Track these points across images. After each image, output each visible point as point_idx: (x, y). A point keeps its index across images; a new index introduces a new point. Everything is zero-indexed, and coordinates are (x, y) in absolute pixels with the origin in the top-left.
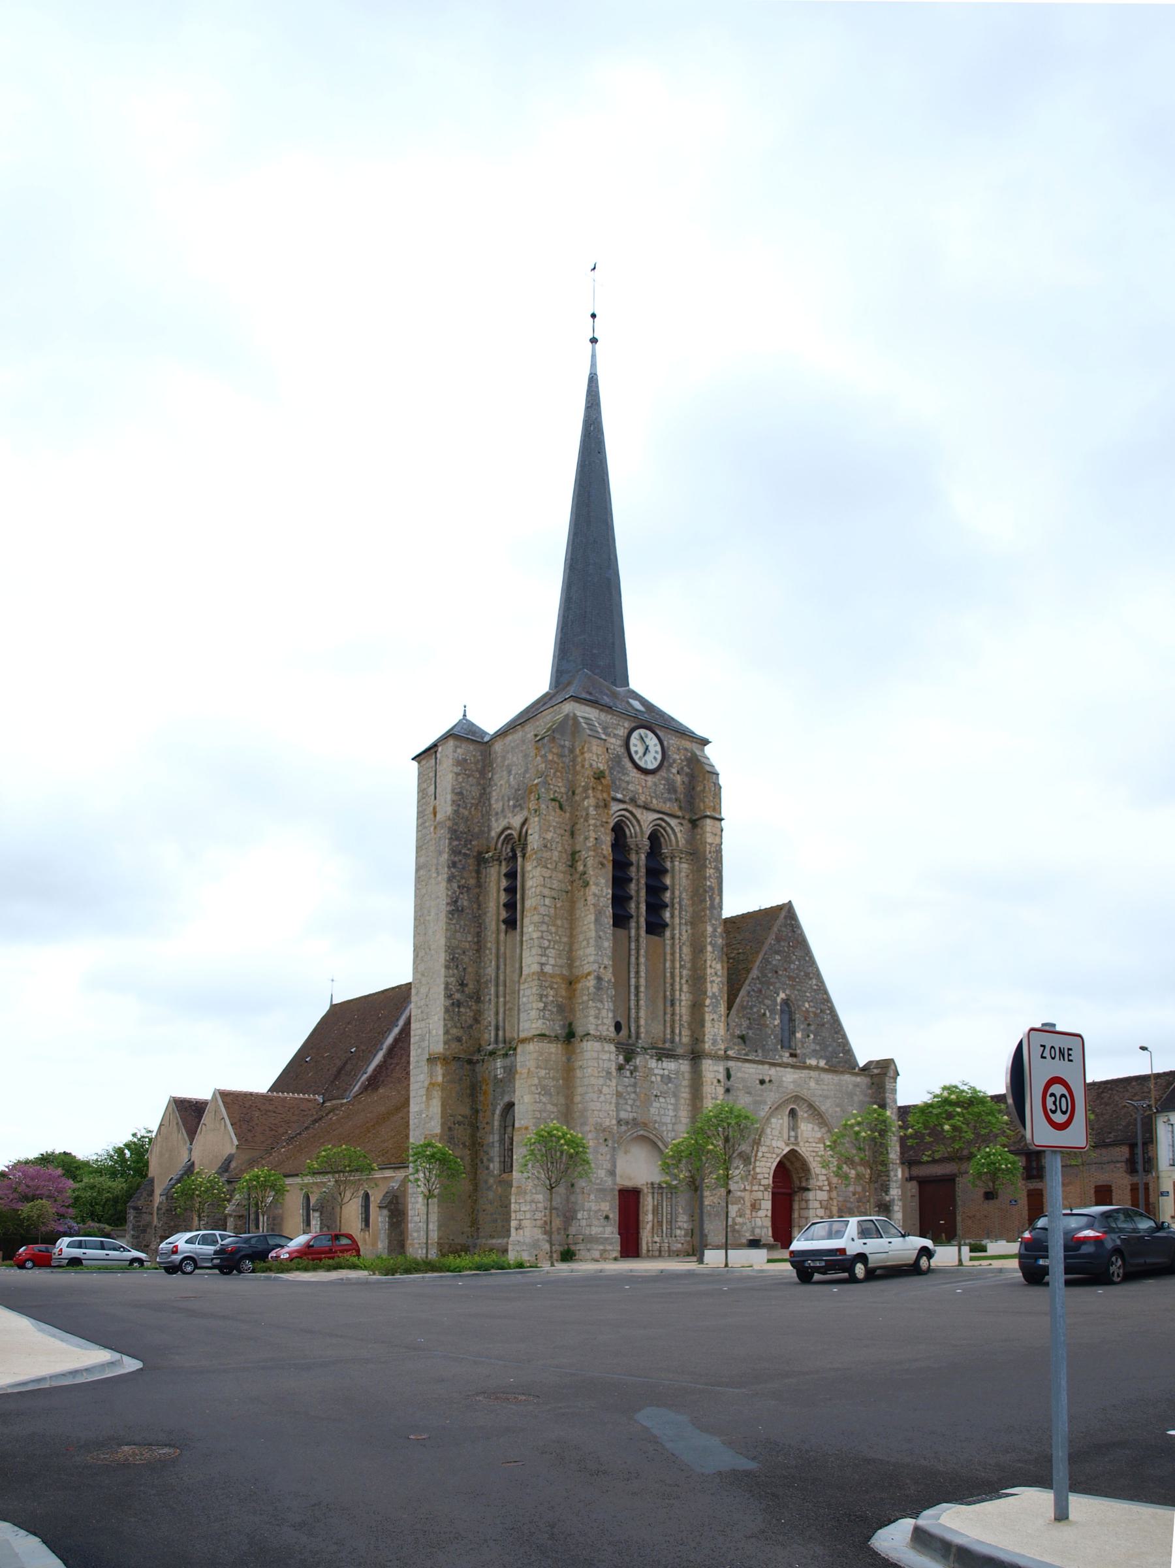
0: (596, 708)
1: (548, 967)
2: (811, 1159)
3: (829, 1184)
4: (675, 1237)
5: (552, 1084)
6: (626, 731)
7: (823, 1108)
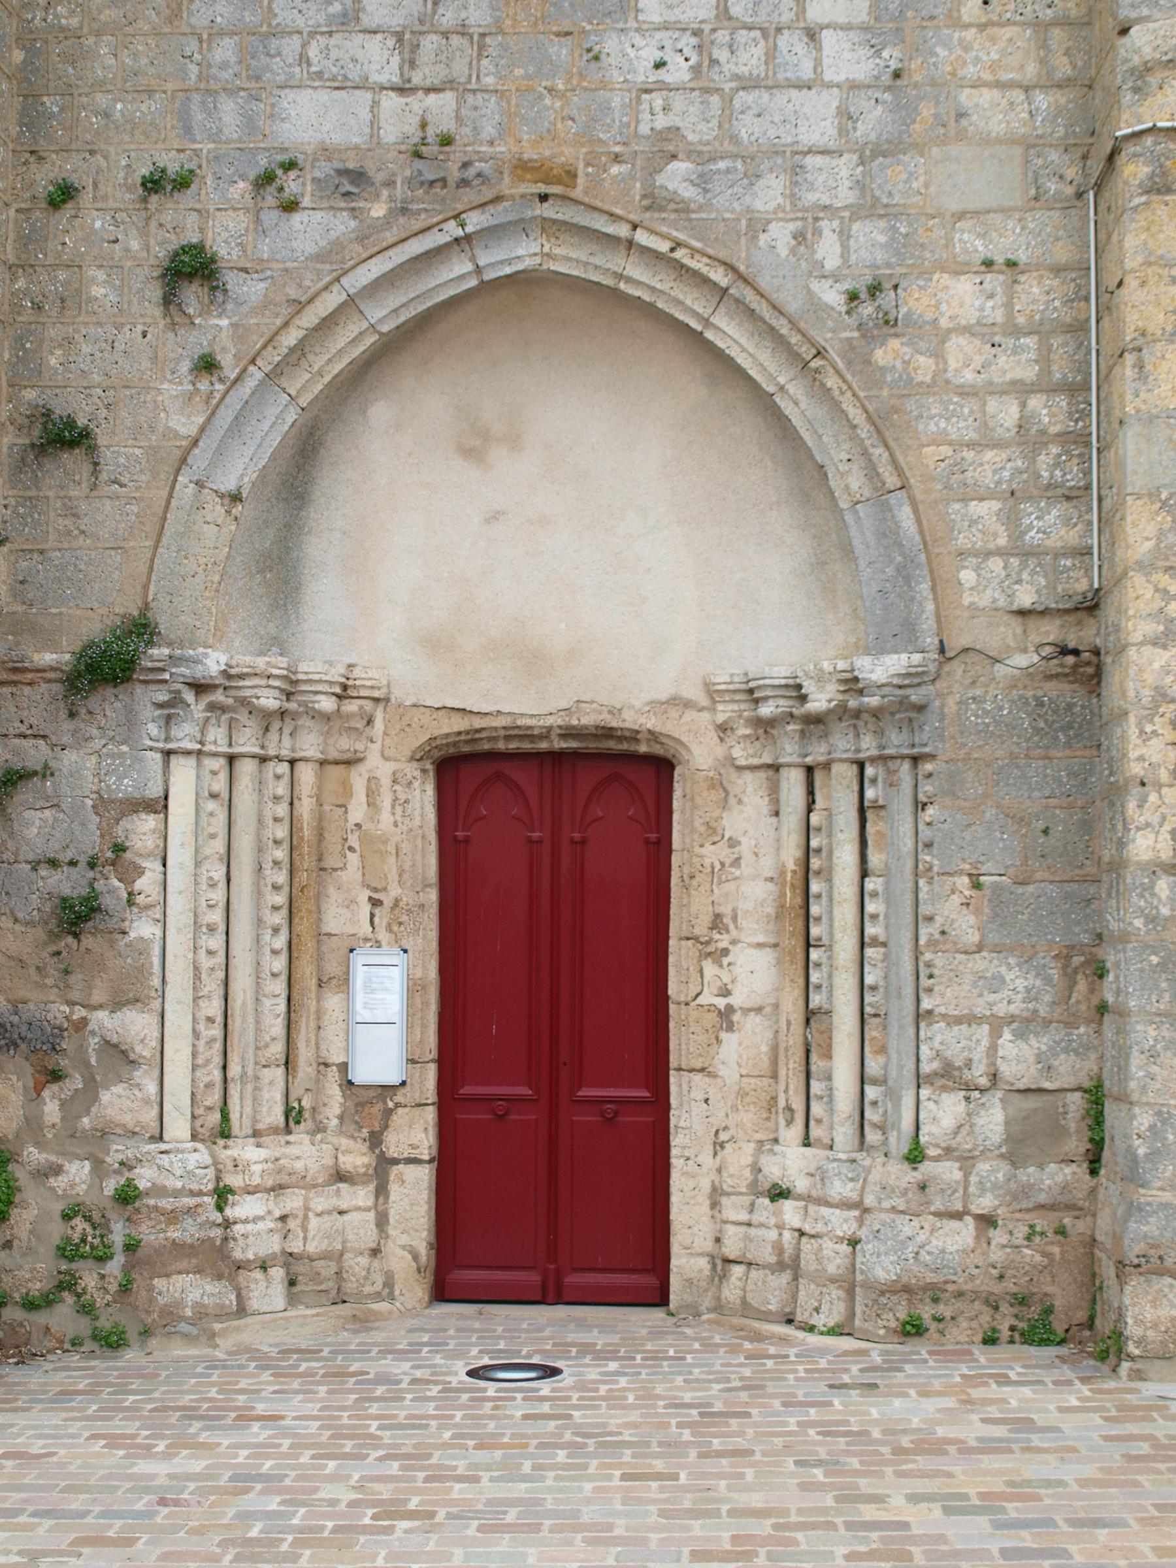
4: (915, 1156)
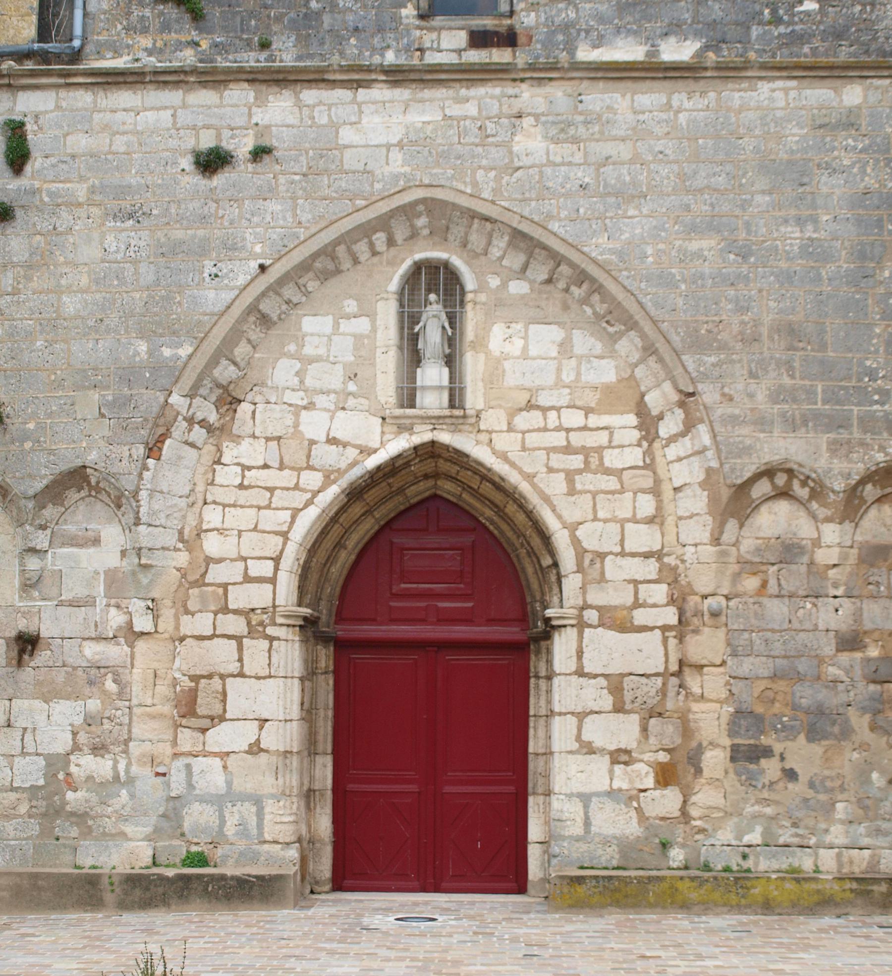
2: (556, 485)
3: (677, 601)
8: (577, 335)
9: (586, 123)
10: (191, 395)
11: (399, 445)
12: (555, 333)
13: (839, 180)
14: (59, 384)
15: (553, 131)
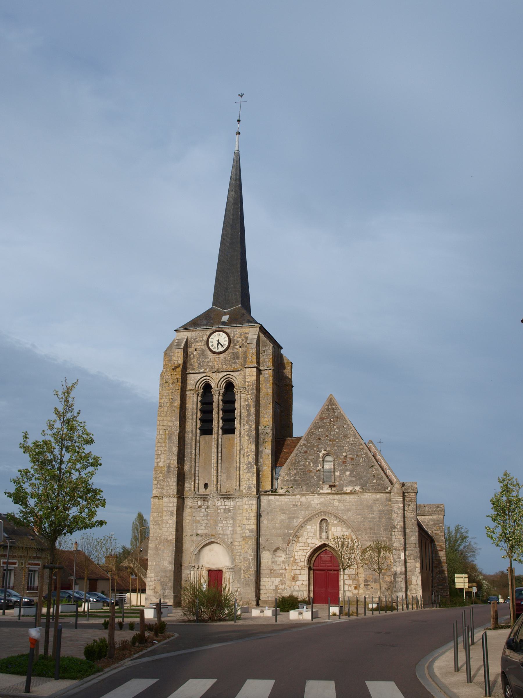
0: (189, 331)
1: (160, 463)
5: (160, 519)
6: (207, 336)
7: (345, 517)
8: (343, 528)
9: (343, 500)
10: (293, 537)
11: (320, 544)
12: (341, 528)
13: (377, 508)
14: (276, 536)
15: (339, 502)
